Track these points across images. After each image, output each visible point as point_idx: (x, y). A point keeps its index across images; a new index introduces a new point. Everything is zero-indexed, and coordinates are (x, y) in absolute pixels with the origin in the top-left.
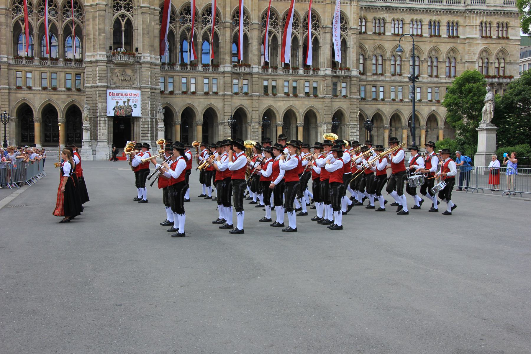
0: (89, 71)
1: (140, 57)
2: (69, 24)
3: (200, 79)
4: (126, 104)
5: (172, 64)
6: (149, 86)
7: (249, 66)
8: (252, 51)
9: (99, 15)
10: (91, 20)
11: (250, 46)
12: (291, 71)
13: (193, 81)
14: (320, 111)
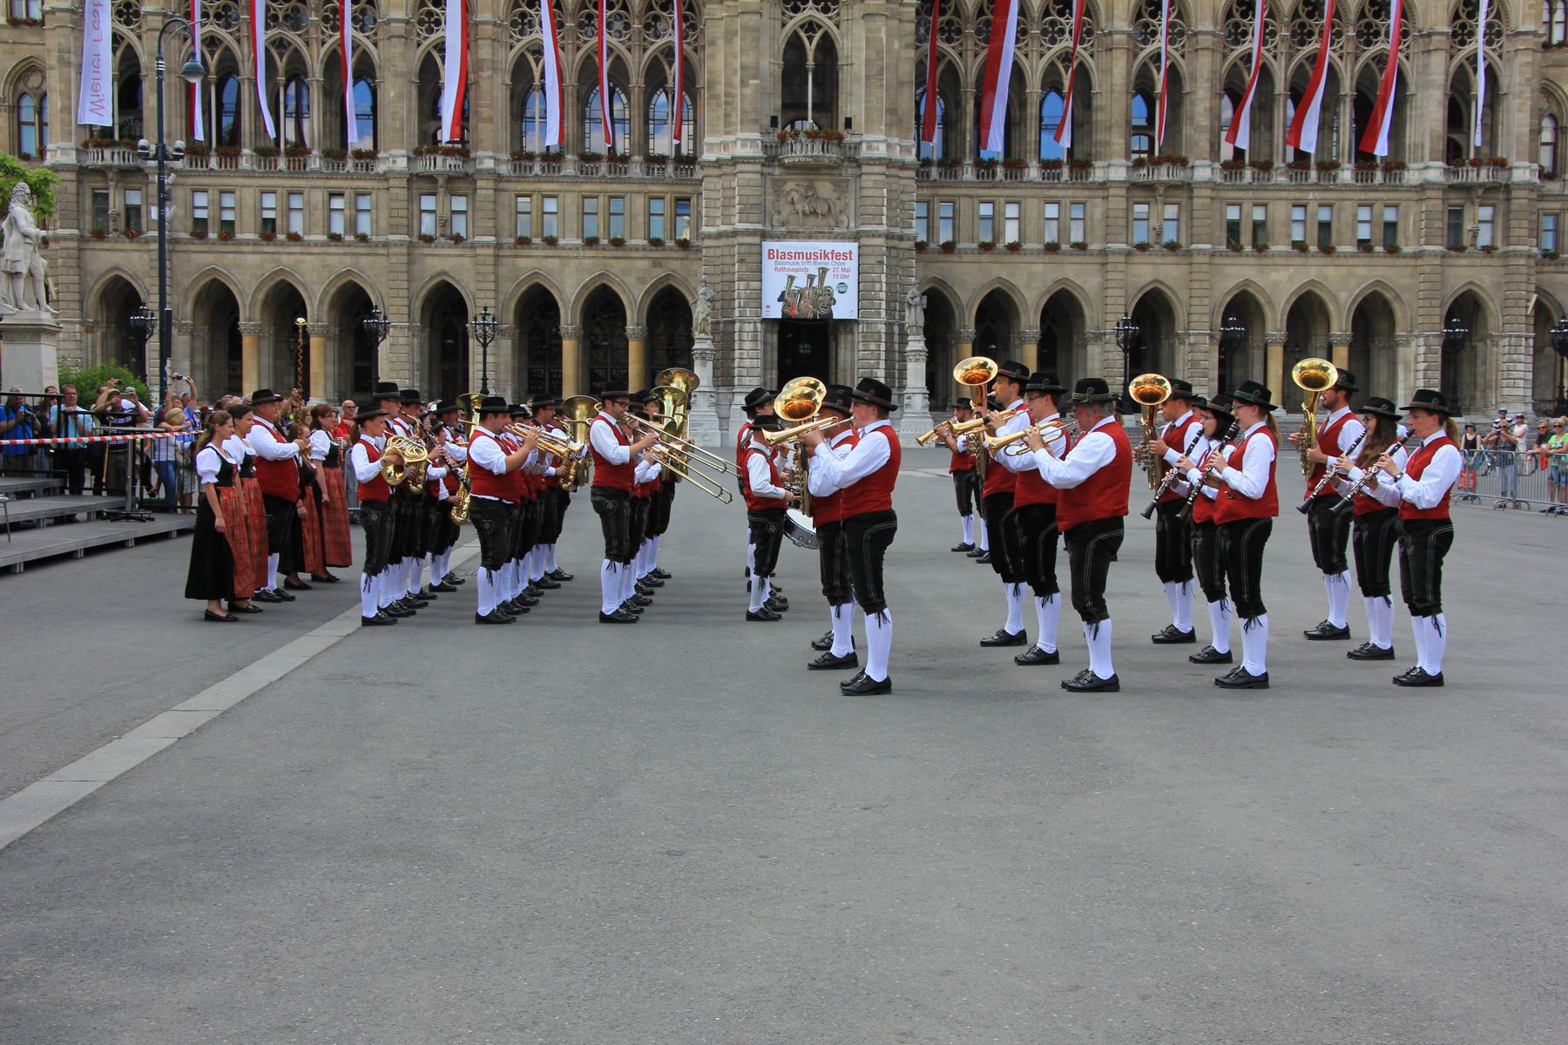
0: (712, 187)
1: (857, 146)
2: (661, 58)
3: (1032, 205)
4: (816, 283)
5: (950, 163)
6: (883, 228)
7: (1183, 162)
8: (1192, 118)
9: (744, 28)
10: (721, 42)
11: (1187, 102)
12: (1313, 174)
13: (1012, 211)
14: (1405, 296)
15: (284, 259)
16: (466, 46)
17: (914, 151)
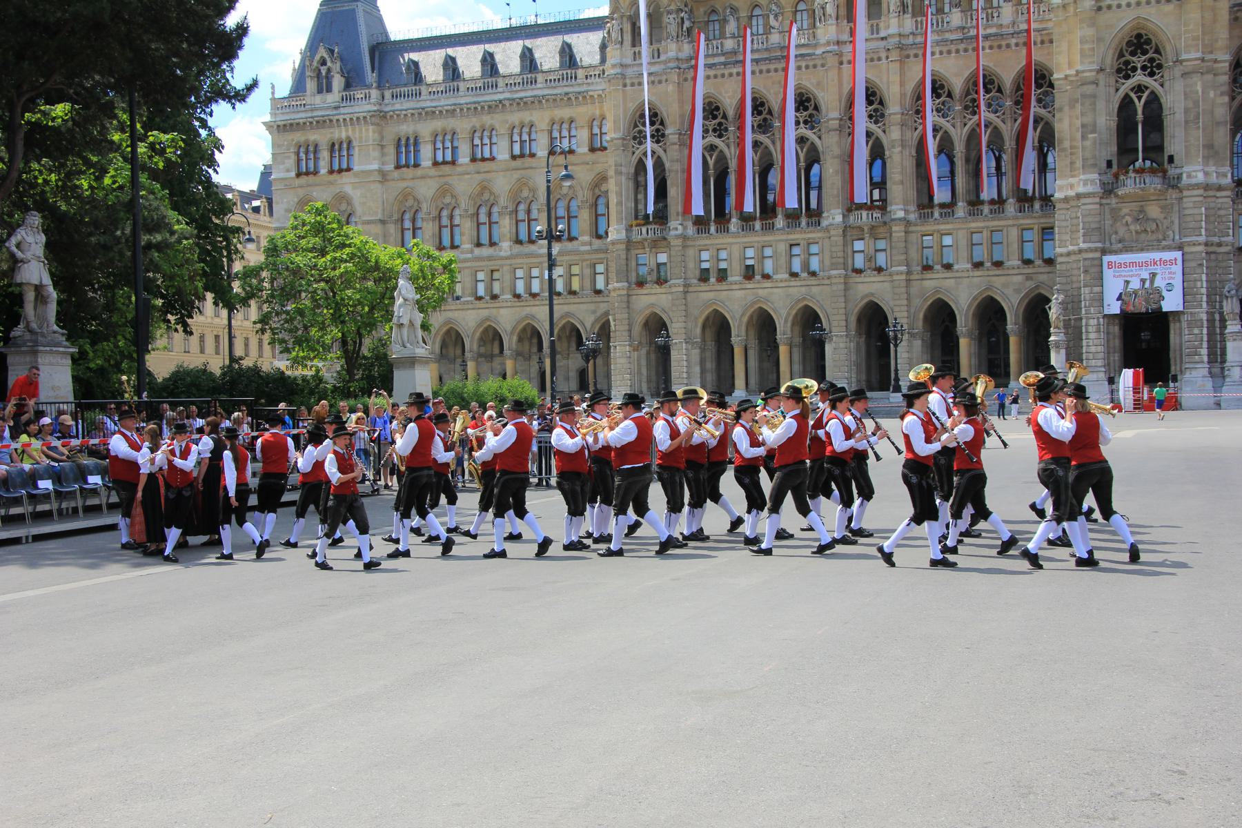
0: (1061, 219)
1: (1179, 177)
4: (1147, 285)
6: (1202, 239)
9: (1084, 96)
10: (1066, 109)
15: (760, 292)
17: (1229, 175)
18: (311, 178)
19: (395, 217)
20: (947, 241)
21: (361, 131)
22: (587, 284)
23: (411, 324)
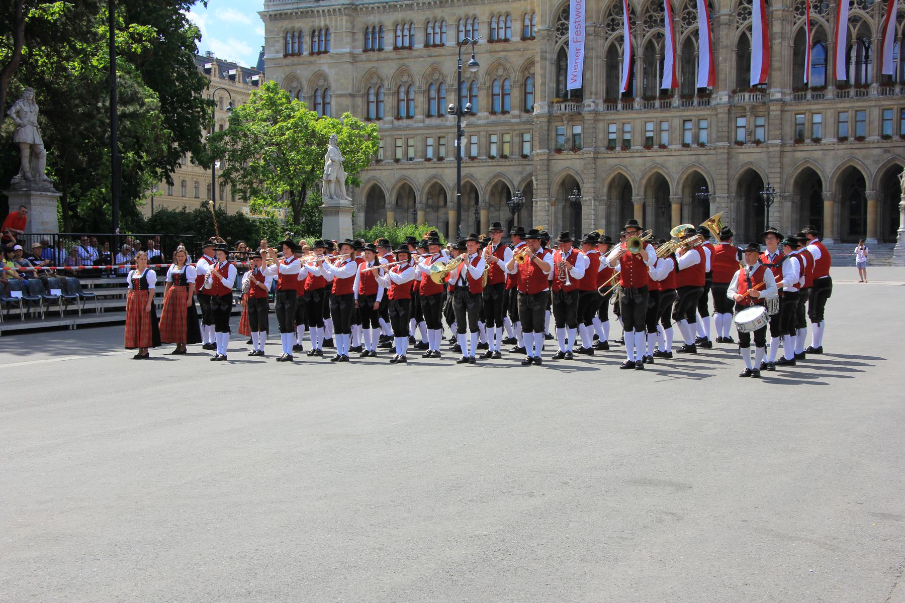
16: (711, 30)
18: (295, 59)
19: (362, 92)
20: (817, 119)
21: (336, 20)
22: (516, 150)
23: (338, 181)
